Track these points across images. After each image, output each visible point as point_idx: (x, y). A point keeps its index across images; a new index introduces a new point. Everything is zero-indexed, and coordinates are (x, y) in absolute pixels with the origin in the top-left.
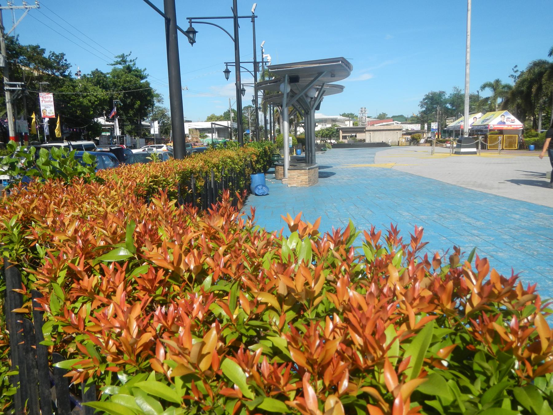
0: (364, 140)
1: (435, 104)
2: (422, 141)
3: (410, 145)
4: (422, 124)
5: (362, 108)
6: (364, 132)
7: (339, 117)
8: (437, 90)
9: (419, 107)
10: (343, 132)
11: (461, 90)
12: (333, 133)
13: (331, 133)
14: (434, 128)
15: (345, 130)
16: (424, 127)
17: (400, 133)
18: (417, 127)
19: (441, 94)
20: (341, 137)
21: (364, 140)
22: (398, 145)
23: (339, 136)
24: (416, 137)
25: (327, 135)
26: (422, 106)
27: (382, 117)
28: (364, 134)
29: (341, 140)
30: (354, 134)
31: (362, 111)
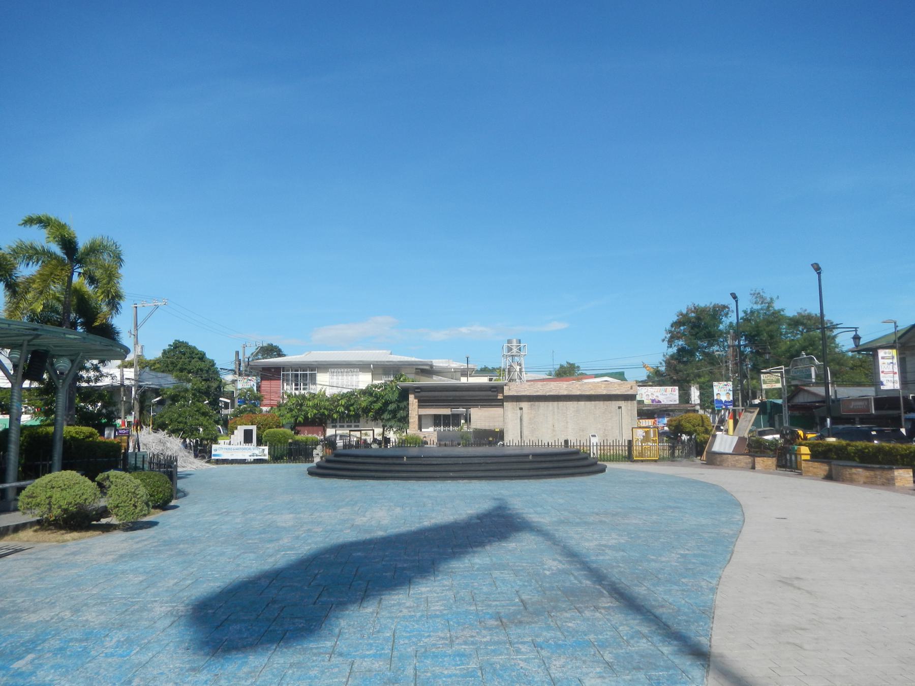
0: (500, 435)
2: (724, 442)
3: (672, 458)
4: (683, 386)
5: (509, 341)
6: (499, 403)
7: (439, 363)
8: (705, 301)
10: (423, 403)
12: (386, 404)
14: (724, 398)
15: (428, 397)
17: (629, 409)
18: (669, 395)
19: (717, 312)
21: (500, 435)
22: (629, 458)
23: (405, 420)
24: (688, 427)
25: (366, 410)
26: (670, 342)
27: (566, 372)
29: (412, 430)
30: (462, 410)
31: (510, 349)
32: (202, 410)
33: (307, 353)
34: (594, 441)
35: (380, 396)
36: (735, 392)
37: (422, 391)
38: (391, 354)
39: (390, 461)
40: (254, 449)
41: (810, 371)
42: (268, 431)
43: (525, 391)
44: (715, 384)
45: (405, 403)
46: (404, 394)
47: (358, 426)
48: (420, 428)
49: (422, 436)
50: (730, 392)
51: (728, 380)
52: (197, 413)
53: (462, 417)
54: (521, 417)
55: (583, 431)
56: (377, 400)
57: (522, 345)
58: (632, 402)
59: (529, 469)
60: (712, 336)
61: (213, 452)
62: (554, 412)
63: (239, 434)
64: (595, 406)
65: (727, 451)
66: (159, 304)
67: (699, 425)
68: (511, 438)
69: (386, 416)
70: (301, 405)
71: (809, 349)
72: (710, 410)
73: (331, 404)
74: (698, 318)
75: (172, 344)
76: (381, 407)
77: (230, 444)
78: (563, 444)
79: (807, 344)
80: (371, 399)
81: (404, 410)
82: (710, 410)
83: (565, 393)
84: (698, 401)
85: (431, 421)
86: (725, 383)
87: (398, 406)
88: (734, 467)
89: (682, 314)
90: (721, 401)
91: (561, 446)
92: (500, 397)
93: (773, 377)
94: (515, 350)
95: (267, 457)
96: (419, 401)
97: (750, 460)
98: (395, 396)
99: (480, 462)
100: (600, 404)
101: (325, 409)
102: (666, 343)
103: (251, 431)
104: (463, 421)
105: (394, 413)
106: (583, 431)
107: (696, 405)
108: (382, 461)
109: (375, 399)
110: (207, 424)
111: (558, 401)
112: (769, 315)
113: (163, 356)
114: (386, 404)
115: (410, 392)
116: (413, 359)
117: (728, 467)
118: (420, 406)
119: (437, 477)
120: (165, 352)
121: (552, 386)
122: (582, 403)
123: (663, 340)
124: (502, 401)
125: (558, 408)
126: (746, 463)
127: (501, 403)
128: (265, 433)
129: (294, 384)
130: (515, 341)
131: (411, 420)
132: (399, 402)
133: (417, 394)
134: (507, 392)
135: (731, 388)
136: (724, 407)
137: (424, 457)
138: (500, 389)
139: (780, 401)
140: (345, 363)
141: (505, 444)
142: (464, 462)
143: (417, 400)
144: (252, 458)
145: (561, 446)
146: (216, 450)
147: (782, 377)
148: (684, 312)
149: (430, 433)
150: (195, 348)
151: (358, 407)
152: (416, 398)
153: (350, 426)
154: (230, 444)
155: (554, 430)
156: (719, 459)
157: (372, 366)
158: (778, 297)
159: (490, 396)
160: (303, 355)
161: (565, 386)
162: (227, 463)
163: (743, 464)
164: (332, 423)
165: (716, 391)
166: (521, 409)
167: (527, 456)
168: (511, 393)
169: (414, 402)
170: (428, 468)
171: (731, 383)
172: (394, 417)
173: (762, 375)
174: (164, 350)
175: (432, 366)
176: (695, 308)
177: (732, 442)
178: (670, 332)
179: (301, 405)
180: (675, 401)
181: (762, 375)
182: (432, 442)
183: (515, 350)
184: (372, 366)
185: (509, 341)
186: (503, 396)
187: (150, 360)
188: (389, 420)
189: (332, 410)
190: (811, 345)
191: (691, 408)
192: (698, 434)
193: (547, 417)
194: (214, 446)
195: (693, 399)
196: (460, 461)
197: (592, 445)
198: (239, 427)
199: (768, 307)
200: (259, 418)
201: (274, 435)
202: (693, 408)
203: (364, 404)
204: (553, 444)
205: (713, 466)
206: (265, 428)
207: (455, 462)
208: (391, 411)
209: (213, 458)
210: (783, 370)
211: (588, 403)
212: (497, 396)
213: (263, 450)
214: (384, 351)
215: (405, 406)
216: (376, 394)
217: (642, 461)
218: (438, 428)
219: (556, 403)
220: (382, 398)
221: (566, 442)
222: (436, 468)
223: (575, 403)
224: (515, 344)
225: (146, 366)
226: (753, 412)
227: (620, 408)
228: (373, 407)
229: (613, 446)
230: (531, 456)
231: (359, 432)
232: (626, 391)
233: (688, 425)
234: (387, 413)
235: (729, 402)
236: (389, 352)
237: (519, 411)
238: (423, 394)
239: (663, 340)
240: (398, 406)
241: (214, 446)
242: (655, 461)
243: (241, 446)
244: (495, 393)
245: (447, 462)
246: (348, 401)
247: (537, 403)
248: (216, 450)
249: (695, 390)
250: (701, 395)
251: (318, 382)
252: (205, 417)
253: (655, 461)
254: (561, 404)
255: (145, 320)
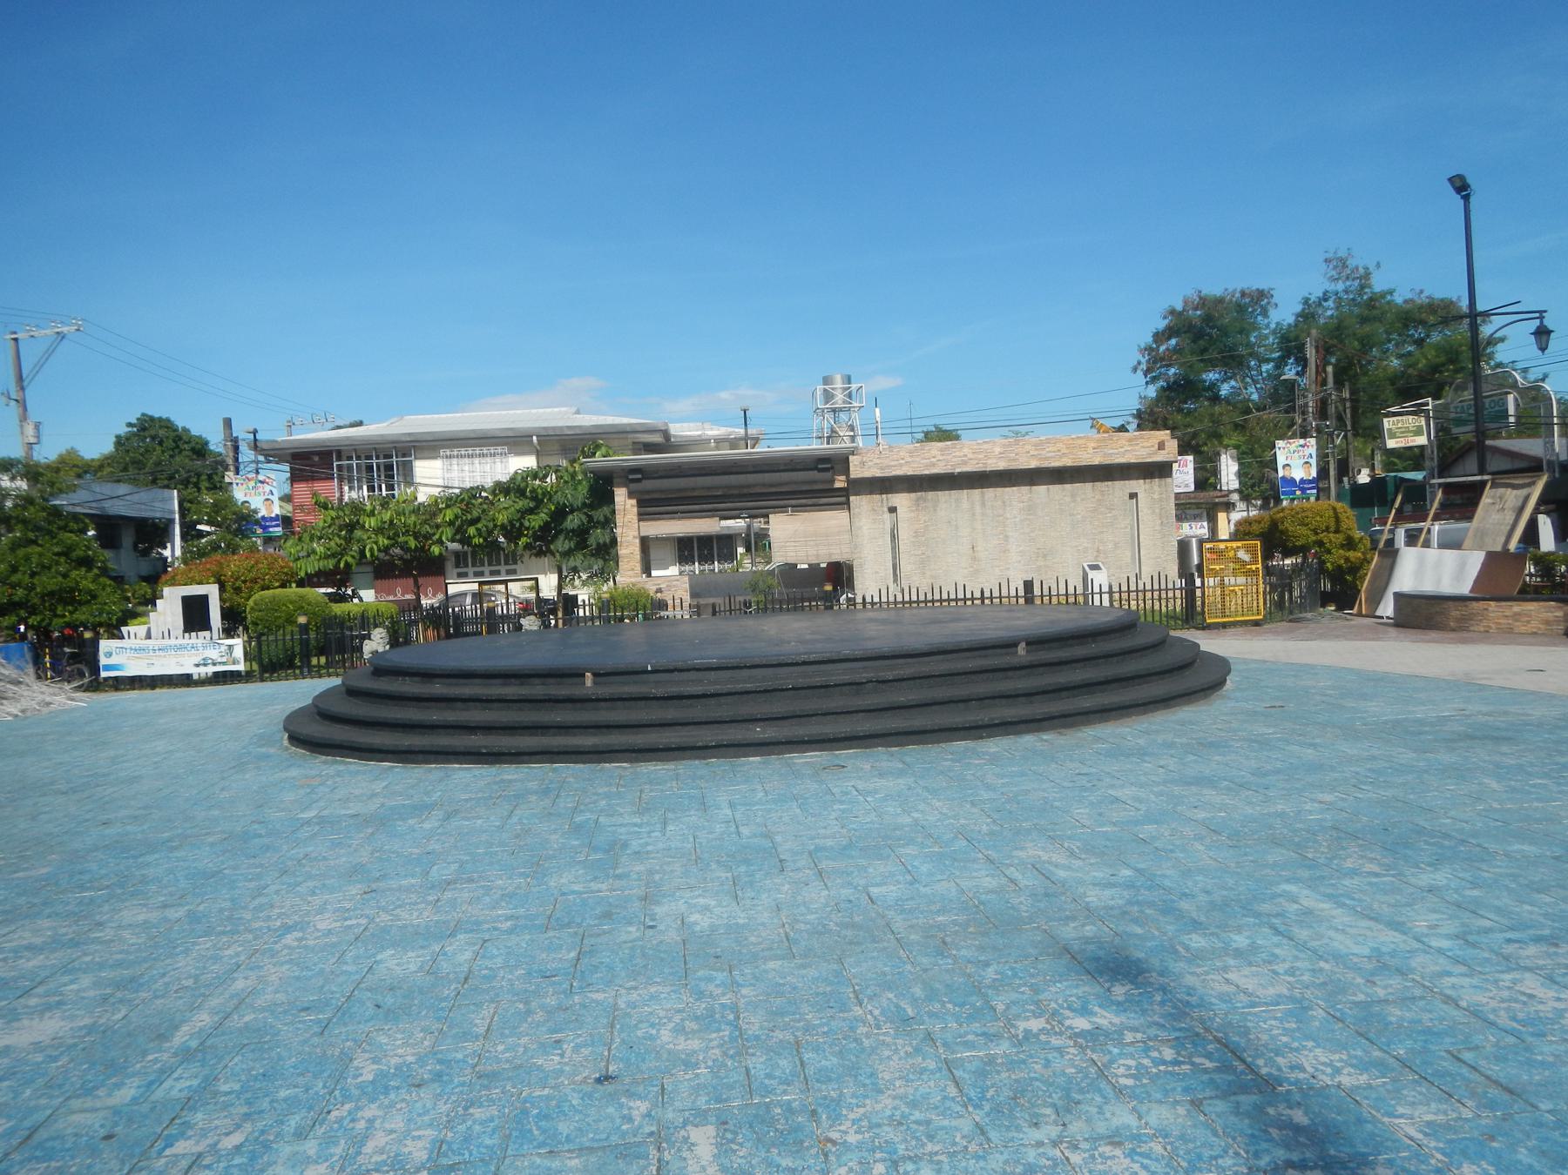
0: (839, 575)
1: (1211, 364)
5: (827, 380)
6: (839, 499)
8: (1222, 282)
9: (1140, 378)
10: (650, 507)
11: (1367, 275)
12: (560, 513)
13: (541, 518)
14: (1298, 474)
16: (1216, 472)
20: (629, 550)
21: (839, 575)
23: (607, 552)
24: (1303, 535)
25: (513, 532)
28: (831, 520)
29: (628, 574)
31: (828, 396)
32: (79, 553)
33: (395, 419)
34: (1100, 579)
35: (544, 494)
36: (1322, 457)
37: (644, 478)
38: (578, 412)
39: (537, 690)
40: (205, 648)
41: (1505, 403)
42: (258, 595)
43: (901, 465)
44: (1280, 443)
45: (606, 510)
46: (602, 488)
47: (514, 572)
48: (647, 570)
49: (651, 587)
50: (1310, 460)
51: (1304, 435)
52: (62, 559)
53: (739, 542)
54: (892, 531)
55: (1045, 556)
56: (537, 507)
57: (854, 386)
58: (1163, 481)
59: (1029, 695)
60: (1233, 362)
61: (103, 661)
62: (974, 515)
63: (169, 606)
64: (1073, 496)
65: (1447, 587)
66: (65, 329)
67: (1327, 529)
68: (870, 583)
69: (562, 544)
70: (351, 527)
71: (1448, 370)
72: (1259, 502)
73: (425, 522)
74: (1208, 319)
75: (134, 421)
76: (547, 524)
77: (149, 636)
78: (1021, 593)
79: (1443, 359)
80: (522, 504)
81: (603, 528)
82: (1259, 502)
83: (1001, 465)
84: (1235, 485)
85: (670, 552)
86: (1302, 441)
87: (590, 518)
88: (1508, 635)
89: (1172, 312)
90: (1293, 480)
91: (1017, 597)
92: (840, 483)
93: (1410, 421)
94: (839, 397)
95: (241, 667)
96: (641, 504)
97: (1560, 614)
98: (581, 494)
99: (857, 678)
100: (1086, 490)
101: (406, 533)
102: (1140, 373)
103: (204, 600)
104: (741, 550)
105: (581, 535)
106: (1045, 556)
107: (1230, 492)
108: (511, 691)
109: (532, 505)
110: (92, 587)
111: (982, 487)
112: (1358, 305)
113: (117, 450)
114: (560, 513)
115: (615, 481)
116: (625, 421)
117: (1486, 637)
118: (642, 517)
119: (706, 747)
120: (119, 442)
121: (966, 450)
122: (1041, 490)
123: (1135, 370)
124: (845, 493)
125: (983, 504)
126: (1547, 622)
127: (843, 499)
128: (251, 603)
129: (365, 488)
130: (838, 378)
131: (623, 551)
132: (592, 507)
133: (634, 486)
134: (856, 471)
135: (1313, 450)
136: (1298, 493)
137: (654, 671)
138: (838, 462)
139: (1418, 476)
140: (472, 435)
141: (859, 600)
142: (801, 682)
143: (634, 502)
144: (211, 670)
145: (1017, 597)
146: (109, 655)
147: (1428, 419)
148: (1179, 307)
149: (671, 580)
150: (186, 430)
151: (491, 525)
152: (631, 495)
153: (481, 574)
154: (149, 636)
155: (974, 559)
156: (1455, 613)
157: (535, 438)
158: (1378, 265)
159: (815, 482)
160: (385, 424)
161: (998, 450)
162: (142, 687)
163: (1535, 625)
164: (457, 566)
165: (1281, 460)
166: (893, 510)
167: (1011, 645)
168: (867, 474)
169: (628, 506)
170: (671, 713)
171: (1313, 441)
172: (582, 545)
173: (1385, 420)
174: (118, 437)
175: (666, 434)
176: (1201, 298)
177: (1462, 566)
178: (1149, 349)
179: (351, 527)
180: (1187, 486)
181: (1385, 420)
182: (678, 602)
183: (839, 397)
184: (535, 438)
185: (827, 380)
186: (848, 481)
187: (93, 460)
188: (567, 554)
189: (428, 537)
190: (1451, 361)
191: (1222, 500)
192: (1329, 552)
193: (957, 527)
194: (105, 645)
195: (1224, 480)
196: (788, 678)
197: (1096, 589)
198: (167, 591)
199: (1362, 287)
200: (234, 565)
201: (275, 605)
202: (1225, 499)
203: (502, 518)
204: (996, 594)
205: (1433, 634)
206: (251, 589)
207: (768, 685)
208: (573, 531)
209: (104, 674)
210: (1430, 407)
211: (1056, 490)
212: (833, 481)
213: (230, 647)
214: (563, 409)
215: (605, 517)
216: (534, 491)
217: (1224, 626)
218: (687, 568)
219: (977, 492)
220: (550, 499)
221: (1028, 585)
222: (697, 711)
223: (1025, 489)
224: (839, 384)
225: (86, 472)
226: (1533, 483)
227: (1133, 496)
228: (527, 524)
229: (1152, 590)
230: (1023, 645)
231: (504, 586)
232: (1150, 455)
233: (1303, 531)
234: (561, 538)
235: (1310, 482)
236: (574, 409)
237: (887, 516)
238: (648, 484)
239: (1135, 370)
240: (590, 518)
241: (105, 645)
242: (1256, 623)
243: (173, 642)
244: (828, 475)
245: (740, 687)
246: (466, 511)
247: (931, 495)
248: (109, 655)
249: (1230, 461)
250: (1241, 475)
251: (417, 480)
252: (90, 569)
253: (1256, 623)
254: (990, 493)
255: (39, 366)
